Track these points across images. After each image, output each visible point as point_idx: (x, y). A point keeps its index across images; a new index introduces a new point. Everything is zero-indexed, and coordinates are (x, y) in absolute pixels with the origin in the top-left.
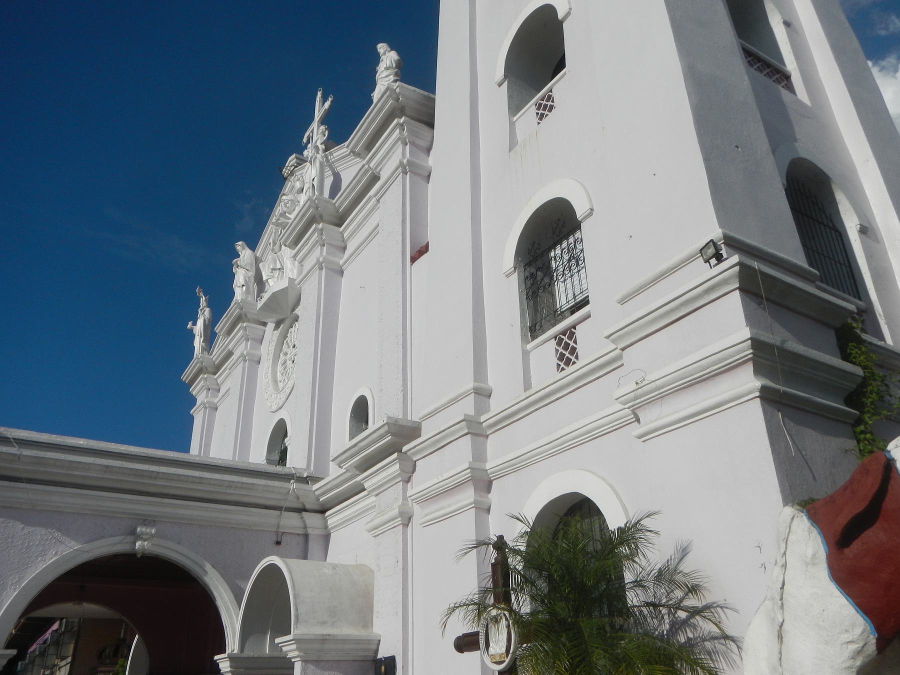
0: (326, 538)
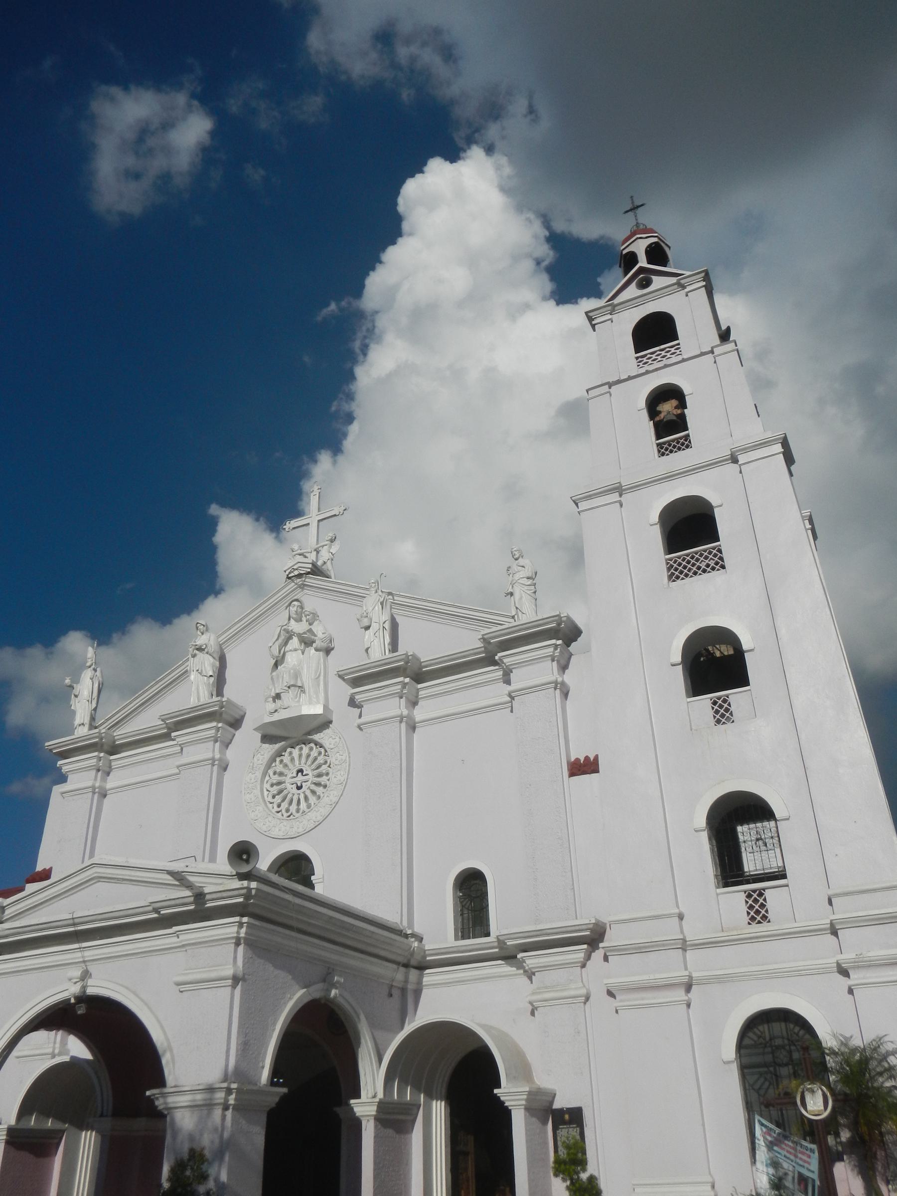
0: (418, 993)
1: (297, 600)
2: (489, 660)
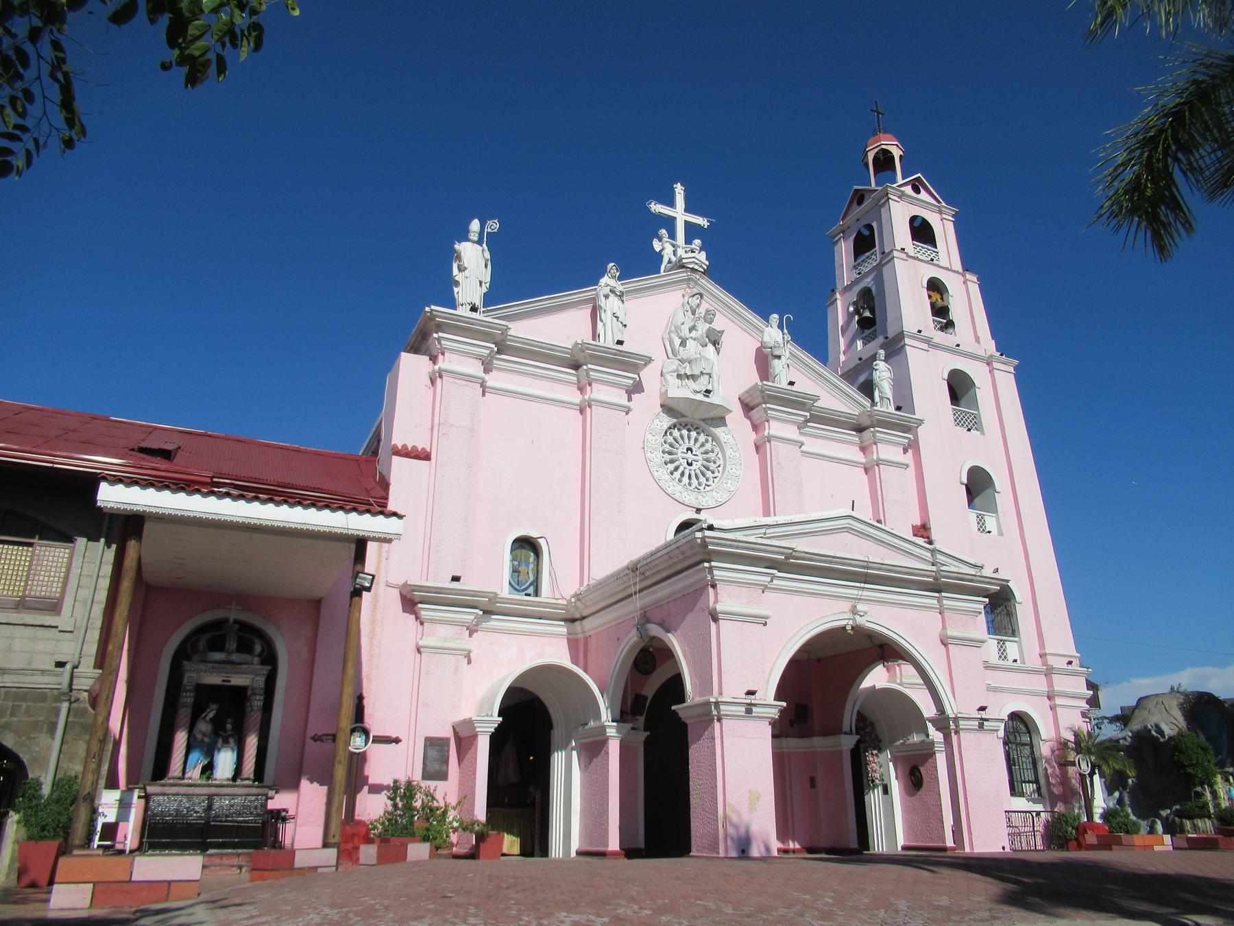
1: (701, 295)
2: (860, 429)
